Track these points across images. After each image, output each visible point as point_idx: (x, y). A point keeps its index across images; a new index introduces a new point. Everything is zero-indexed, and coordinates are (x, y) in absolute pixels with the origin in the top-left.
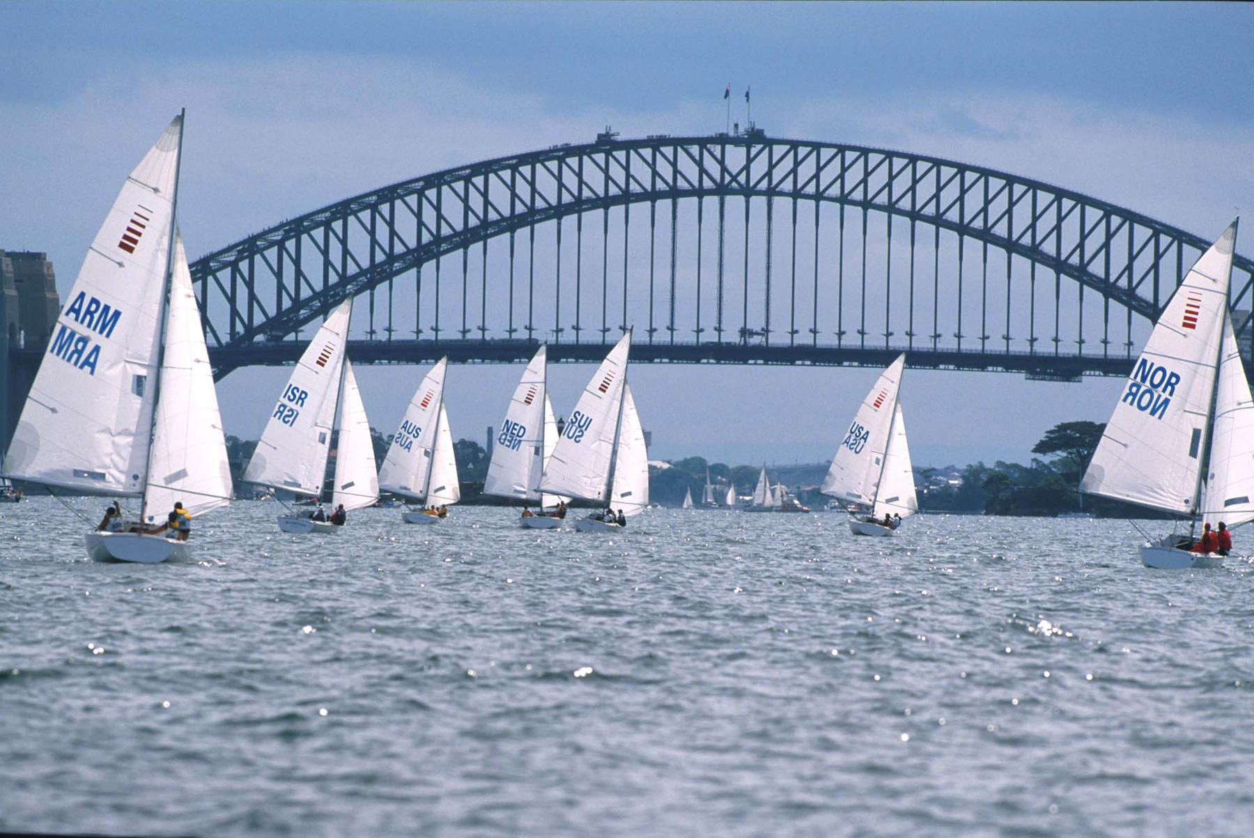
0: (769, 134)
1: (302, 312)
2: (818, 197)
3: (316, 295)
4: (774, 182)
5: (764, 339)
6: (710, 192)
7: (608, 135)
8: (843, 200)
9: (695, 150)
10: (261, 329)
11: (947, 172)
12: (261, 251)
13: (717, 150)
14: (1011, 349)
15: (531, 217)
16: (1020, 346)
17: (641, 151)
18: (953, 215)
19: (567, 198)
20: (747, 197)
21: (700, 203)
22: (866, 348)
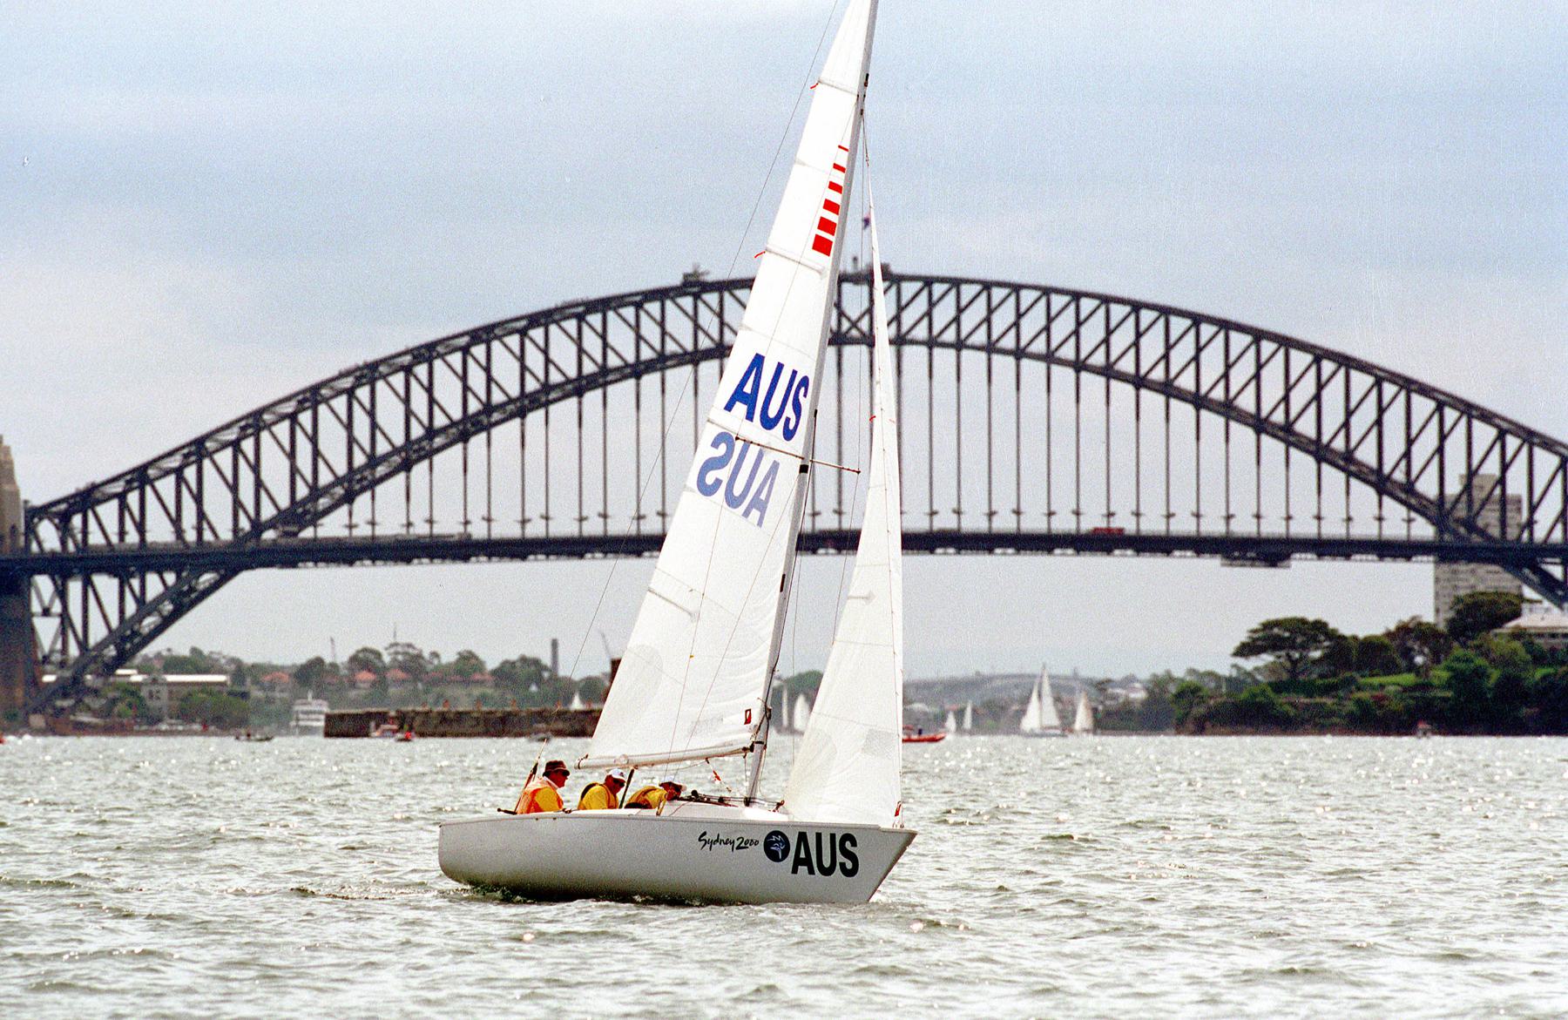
2: (959, 345)
3: (338, 481)
4: (904, 329)
8: (990, 348)
10: (271, 524)
11: (1118, 311)
15: (602, 378)
16: (1213, 526)
18: (1127, 365)
19: (647, 354)
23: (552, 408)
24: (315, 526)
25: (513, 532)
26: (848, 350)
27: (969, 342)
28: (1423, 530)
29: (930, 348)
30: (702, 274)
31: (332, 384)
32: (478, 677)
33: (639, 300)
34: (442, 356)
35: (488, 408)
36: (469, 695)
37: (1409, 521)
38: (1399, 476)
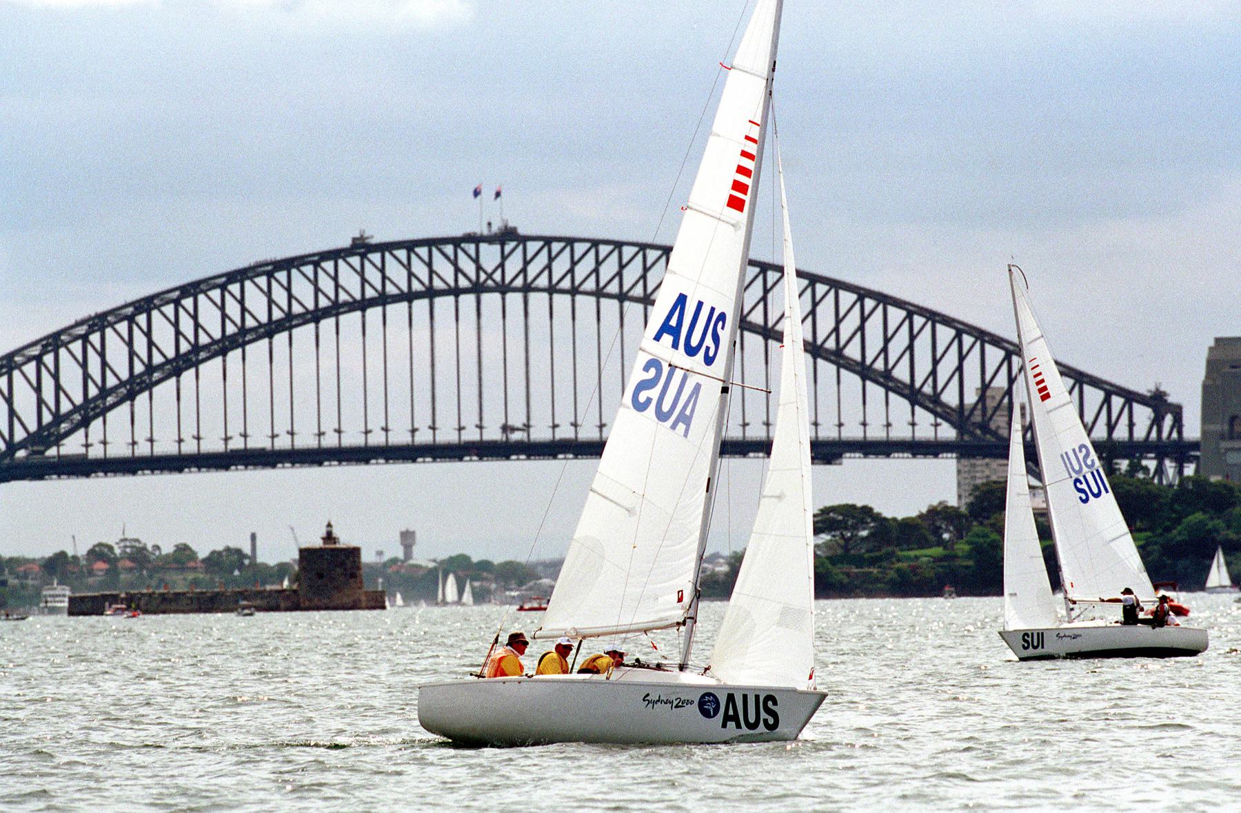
0: (522, 231)
1: (63, 425)
2: (574, 291)
3: (76, 409)
4: (530, 279)
5: (525, 435)
6: (466, 291)
7: (362, 238)
8: (599, 293)
9: (449, 249)
10: (22, 445)
12: (19, 367)
13: (471, 248)
14: (868, 435)
15: (288, 323)
17: (395, 252)
19: (324, 303)
20: (503, 293)
21: (457, 302)
22: (747, 439)
23: (248, 348)
24: (58, 446)
25: (218, 447)
26: (485, 297)
27: (582, 288)
28: (948, 432)
29: (551, 295)
30: (367, 238)
31: (71, 331)
32: (192, 564)
33: (317, 259)
34: (158, 308)
35: (196, 348)
36: (185, 579)
37: (936, 425)
38: (928, 389)
